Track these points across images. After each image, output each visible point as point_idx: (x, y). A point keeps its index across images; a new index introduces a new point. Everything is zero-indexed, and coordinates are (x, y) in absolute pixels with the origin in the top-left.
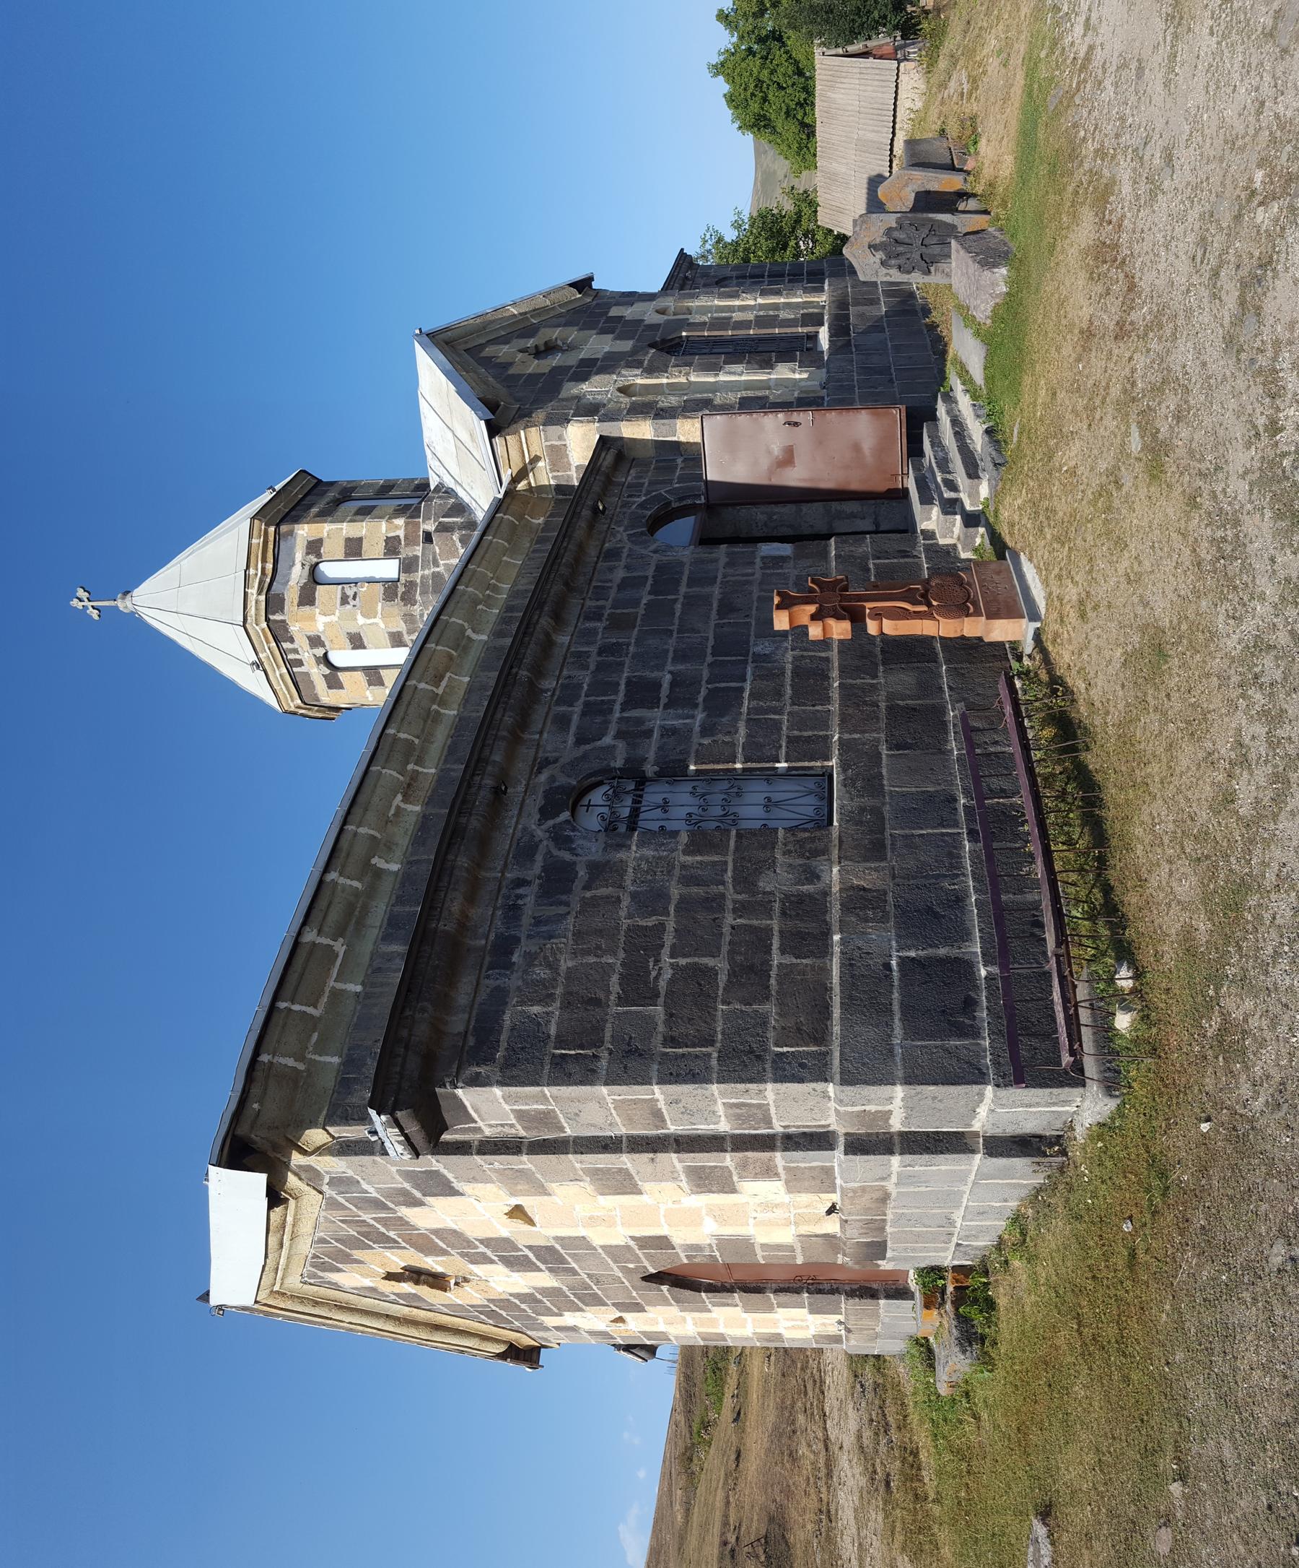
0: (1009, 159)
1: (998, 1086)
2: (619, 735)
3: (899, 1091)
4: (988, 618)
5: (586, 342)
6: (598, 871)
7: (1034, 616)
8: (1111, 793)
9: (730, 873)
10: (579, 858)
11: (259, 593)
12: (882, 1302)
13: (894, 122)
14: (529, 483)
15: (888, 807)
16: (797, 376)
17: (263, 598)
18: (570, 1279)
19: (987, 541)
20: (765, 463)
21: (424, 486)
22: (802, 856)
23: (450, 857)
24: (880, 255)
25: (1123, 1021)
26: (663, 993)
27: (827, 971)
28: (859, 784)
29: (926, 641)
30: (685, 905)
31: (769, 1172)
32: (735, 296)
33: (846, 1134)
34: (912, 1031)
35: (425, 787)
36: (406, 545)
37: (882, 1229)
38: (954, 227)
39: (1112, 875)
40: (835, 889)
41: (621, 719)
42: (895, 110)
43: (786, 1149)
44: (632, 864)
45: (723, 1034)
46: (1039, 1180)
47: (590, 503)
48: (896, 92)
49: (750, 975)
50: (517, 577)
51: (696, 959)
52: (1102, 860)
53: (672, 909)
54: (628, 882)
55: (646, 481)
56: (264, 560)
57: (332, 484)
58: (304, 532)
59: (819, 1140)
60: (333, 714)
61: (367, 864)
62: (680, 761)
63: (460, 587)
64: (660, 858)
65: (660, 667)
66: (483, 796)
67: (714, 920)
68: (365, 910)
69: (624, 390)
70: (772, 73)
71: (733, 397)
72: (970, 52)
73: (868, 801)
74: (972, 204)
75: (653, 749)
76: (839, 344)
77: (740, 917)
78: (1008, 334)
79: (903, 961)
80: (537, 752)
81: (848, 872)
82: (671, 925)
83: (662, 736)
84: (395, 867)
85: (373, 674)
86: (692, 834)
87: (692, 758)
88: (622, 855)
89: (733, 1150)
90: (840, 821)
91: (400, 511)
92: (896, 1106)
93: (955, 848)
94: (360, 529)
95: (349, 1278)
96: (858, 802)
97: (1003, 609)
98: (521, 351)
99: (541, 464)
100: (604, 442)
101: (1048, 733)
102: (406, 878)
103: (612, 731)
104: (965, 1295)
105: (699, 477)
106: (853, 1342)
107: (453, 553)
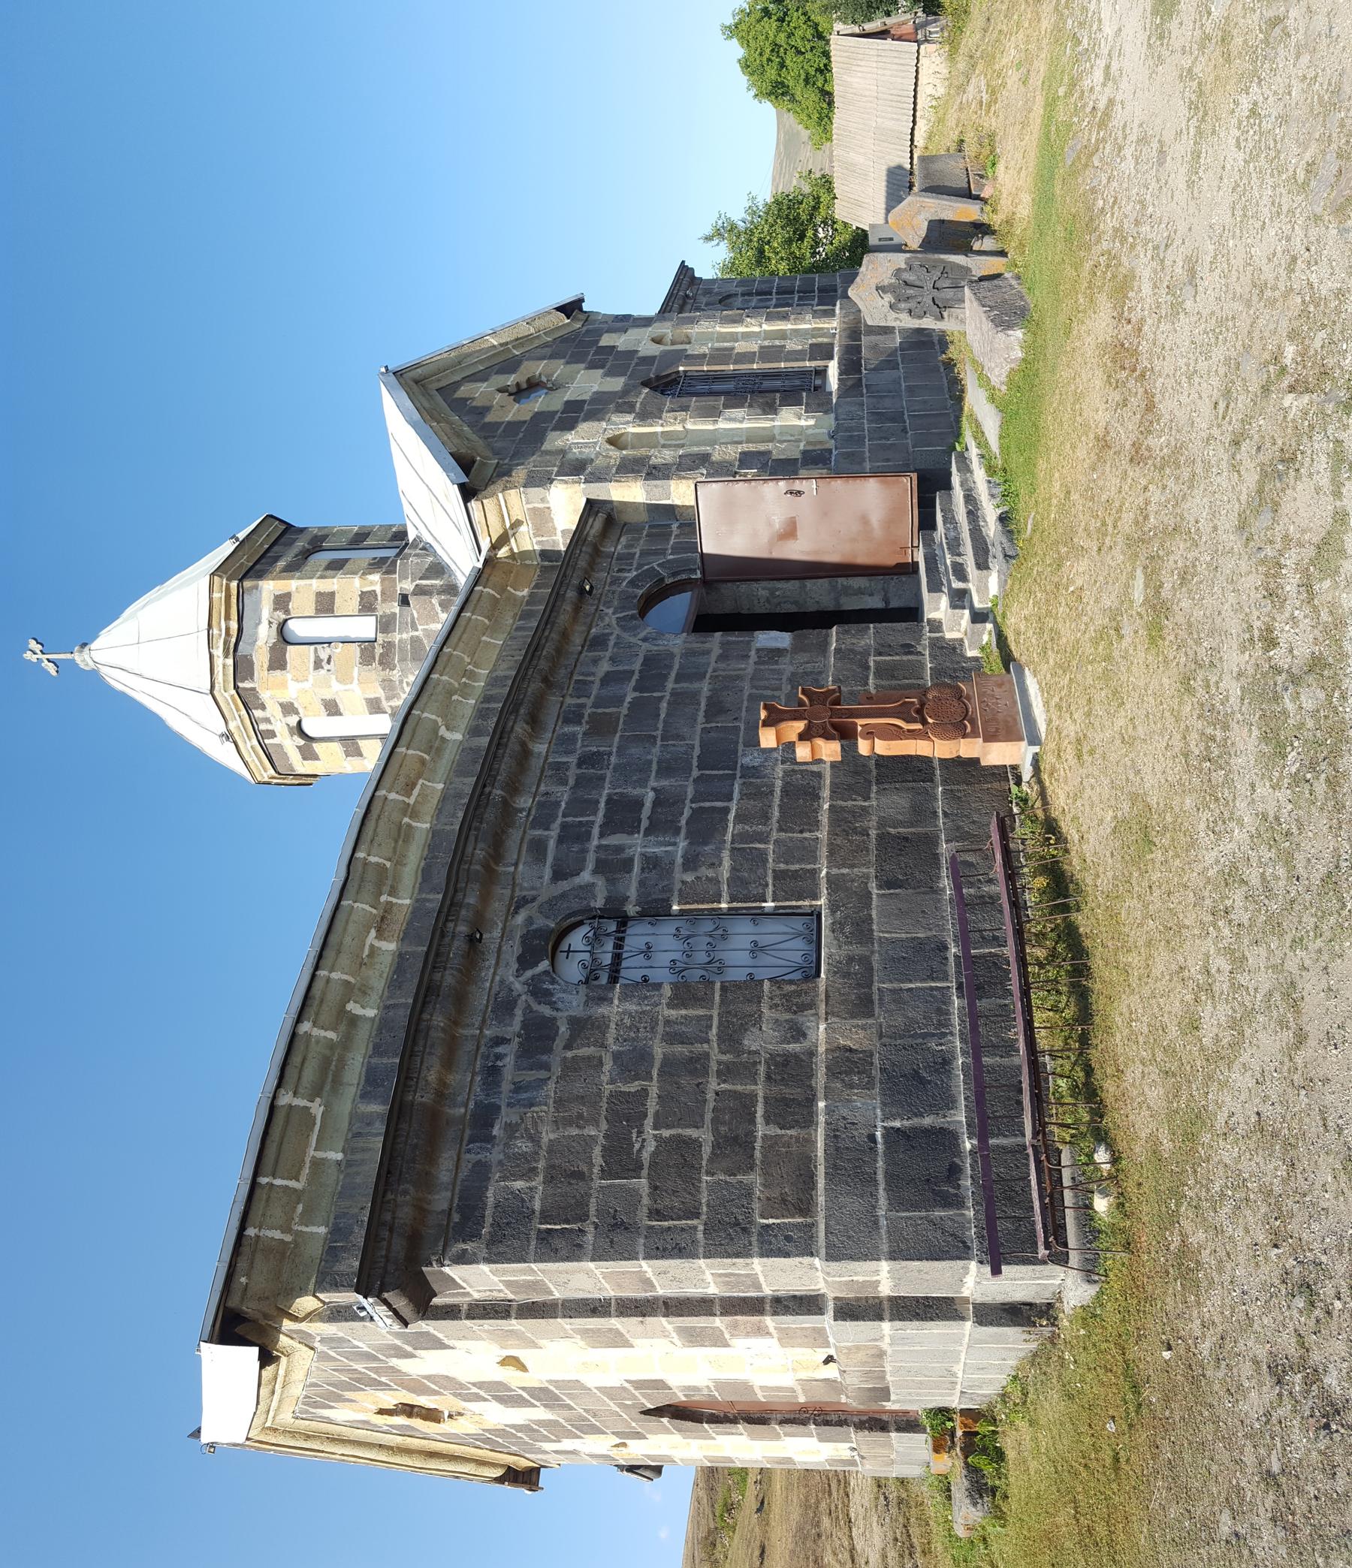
0: (1026, 198)
1: (981, 1262)
3: (884, 1266)
4: (985, 741)
5: (573, 379)
6: (578, 1026)
7: (1034, 740)
8: (1096, 963)
9: (714, 1031)
10: (560, 1014)
11: (226, 656)
12: (893, 1435)
13: (915, 110)
14: (511, 549)
15: (876, 957)
16: (803, 423)
17: (230, 661)
18: (566, 1413)
19: (994, 639)
20: (764, 536)
21: (402, 534)
22: (789, 1010)
23: (425, 1016)
24: (889, 298)
25: (1101, 1204)
27: (813, 1143)
28: (847, 929)
29: (927, 761)
31: (761, 1331)
32: (737, 321)
33: (836, 1299)
34: (897, 1202)
35: (399, 921)
36: (384, 601)
37: (883, 1378)
38: (968, 270)
39: (1094, 1055)
40: (822, 1049)
41: (599, 847)
42: (915, 97)
43: (775, 1313)
44: (614, 1019)
45: (708, 1206)
46: (1033, 1346)
47: (575, 582)
48: (916, 78)
49: (735, 1146)
50: (497, 660)
51: (680, 1131)
52: (1084, 1040)
53: (655, 1073)
54: (610, 1041)
55: (637, 551)
56: (228, 618)
57: (302, 530)
58: (269, 587)
59: (807, 1304)
60: (309, 780)
61: (342, 1012)
62: (663, 900)
63: (434, 676)
64: (643, 1012)
66: (457, 947)
67: (698, 1085)
68: (342, 1063)
69: (613, 441)
70: (789, 37)
71: (732, 453)
72: (990, 59)
73: (857, 950)
74: (988, 243)
75: (634, 885)
76: (850, 383)
77: (725, 1081)
78: (1023, 397)
79: (889, 1132)
80: (513, 891)
81: (834, 1030)
82: (654, 1091)
84: (371, 1013)
85: (351, 745)
86: (675, 986)
87: (675, 898)
88: (603, 1010)
89: (722, 1314)
90: (828, 971)
91: (377, 565)
92: (884, 1277)
93: (945, 1003)
94: (332, 584)
95: (341, 1413)
97: (1001, 731)
98: (500, 390)
99: (523, 529)
100: (592, 506)
101: (1041, 882)
102: (383, 1024)
104: (972, 1437)
105: (693, 547)
106: (868, 1467)
107: (434, 619)
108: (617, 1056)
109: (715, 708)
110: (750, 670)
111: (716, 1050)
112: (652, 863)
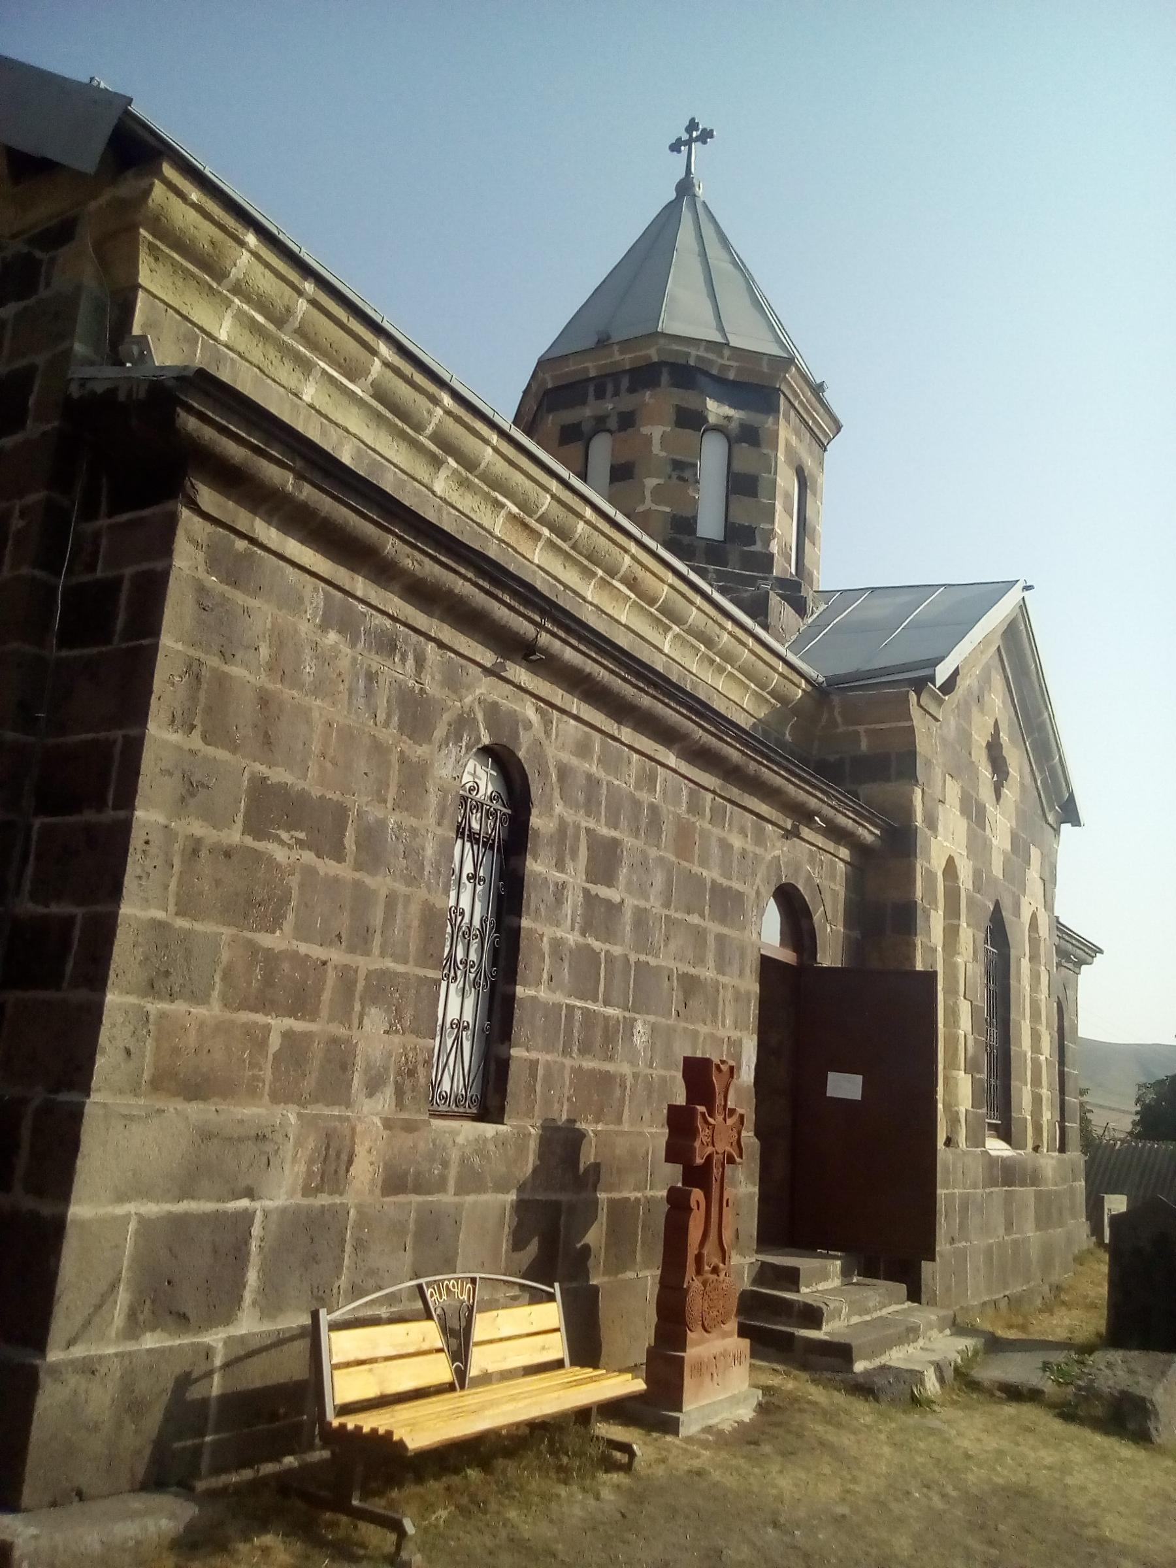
2: (563, 827)
6: (415, 776)
26: (261, 846)
30: (362, 897)
53: (357, 875)
65: (629, 891)
67: (339, 936)
83: (557, 884)
96: (454, 1156)
108: (382, 823)
109: (690, 985)
110: (722, 1033)
111: (372, 967)
112: (561, 887)
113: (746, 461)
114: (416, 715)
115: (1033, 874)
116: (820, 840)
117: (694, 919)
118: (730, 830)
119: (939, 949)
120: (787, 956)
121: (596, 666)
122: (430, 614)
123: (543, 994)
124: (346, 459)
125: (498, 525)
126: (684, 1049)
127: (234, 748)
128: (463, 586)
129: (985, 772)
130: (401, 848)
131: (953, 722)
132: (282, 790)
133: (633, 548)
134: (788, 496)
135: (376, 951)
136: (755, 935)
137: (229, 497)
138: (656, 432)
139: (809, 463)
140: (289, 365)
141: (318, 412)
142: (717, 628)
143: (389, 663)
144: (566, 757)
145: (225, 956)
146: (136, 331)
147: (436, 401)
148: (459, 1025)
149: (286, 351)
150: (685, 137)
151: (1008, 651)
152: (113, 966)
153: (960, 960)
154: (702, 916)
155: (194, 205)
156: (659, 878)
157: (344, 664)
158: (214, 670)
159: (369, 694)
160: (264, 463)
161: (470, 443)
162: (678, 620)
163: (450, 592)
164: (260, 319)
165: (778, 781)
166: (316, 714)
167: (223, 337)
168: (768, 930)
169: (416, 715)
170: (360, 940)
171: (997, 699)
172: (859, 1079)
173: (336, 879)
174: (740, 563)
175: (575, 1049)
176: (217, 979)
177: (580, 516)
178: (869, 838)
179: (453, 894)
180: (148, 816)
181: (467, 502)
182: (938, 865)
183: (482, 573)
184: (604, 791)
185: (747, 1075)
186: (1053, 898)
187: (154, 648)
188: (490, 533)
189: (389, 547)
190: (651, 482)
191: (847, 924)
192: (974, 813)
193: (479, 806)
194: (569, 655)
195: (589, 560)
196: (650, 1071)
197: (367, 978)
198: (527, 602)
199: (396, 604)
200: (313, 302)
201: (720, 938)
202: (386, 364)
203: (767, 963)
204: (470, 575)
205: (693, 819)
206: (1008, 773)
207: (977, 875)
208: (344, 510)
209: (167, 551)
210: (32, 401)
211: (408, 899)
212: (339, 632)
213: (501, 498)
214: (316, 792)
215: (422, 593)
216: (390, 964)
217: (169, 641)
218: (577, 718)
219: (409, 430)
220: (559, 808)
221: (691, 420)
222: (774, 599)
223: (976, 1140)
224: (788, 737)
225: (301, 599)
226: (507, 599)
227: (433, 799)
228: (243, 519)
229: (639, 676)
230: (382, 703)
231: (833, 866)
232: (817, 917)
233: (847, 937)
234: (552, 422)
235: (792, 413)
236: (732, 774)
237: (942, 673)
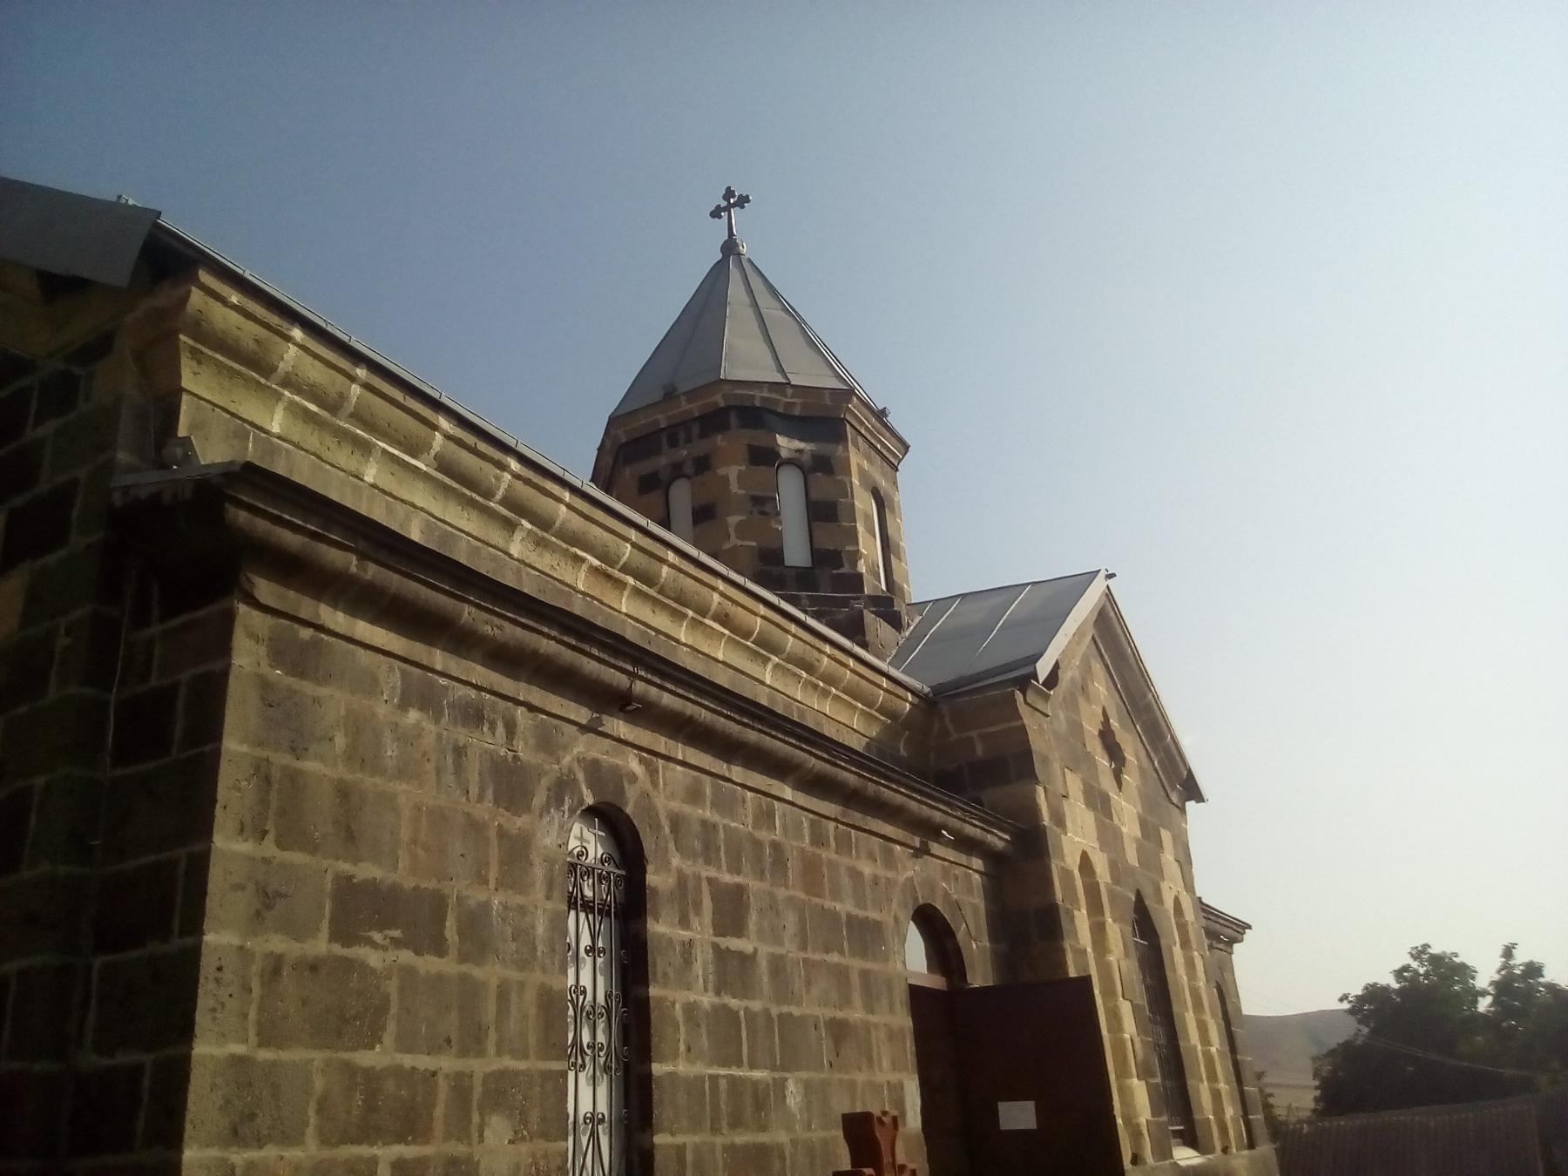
6: (517, 850)
30: (470, 991)
53: (464, 968)
67: (449, 1041)
103: (689, 867)
108: (485, 906)
109: (840, 1031)
113: (823, 488)
114: (511, 785)
115: (1168, 857)
116: (951, 854)
117: (834, 958)
118: (858, 857)
119: (1089, 950)
120: (936, 982)
121: (696, 708)
122: (516, 678)
123: (682, 1068)
124: (415, 535)
125: (581, 580)
126: (842, 1105)
127: (313, 849)
128: (547, 645)
129: (1103, 761)
130: (509, 931)
131: (1062, 716)
132: (371, 887)
133: (721, 585)
134: (868, 518)
135: (491, 1049)
136: (899, 965)
137: (288, 586)
138: (732, 472)
139: (883, 484)
140: (347, 450)
141: (384, 492)
142: (816, 654)
143: (477, 734)
144: (675, 805)
145: (319, 1084)
146: (182, 433)
147: (503, 467)
148: (594, 1119)
149: (343, 436)
150: (724, 204)
151: (1102, 637)
152: (189, 1116)
153: (1112, 958)
154: (842, 953)
155: (234, 307)
156: (791, 920)
157: (428, 741)
158: (285, 768)
159: (459, 769)
160: (323, 548)
161: (542, 503)
162: (776, 650)
163: (535, 653)
164: (313, 407)
165: (899, 799)
166: (402, 799)
167: (276, 429)
168: (913, 956)
169: (511, 785)
170: (472, 1042)
171: (1101, 688)
172: (1030, 1105)
173: (440, 978)
174: (832, 587)
175: (724, 1123)
176: (311, 1112)
177: (663, 561)
178: (1000, 845)
179: (571, 972)
180: (218, 939)
181: (545, 561)
182: (1073, 862)
183: (566, 629)
184: (722, 835)
185: (913, 1120)
186: (1192, 879)
187: (216, 755)
188: (574, 588)
189: (466, 614)
190: (733, 520)
191: (994, 936)
192: (1099, 803)
193: (589, 871)
194: (667, 700)
195: (678, 603)
196: (807, 1135)
197: (485, 1081)
198: (616, 652)
199: (480, 673)
200: (367, 386)
201: (865, 974)
202: (448, 437)
203: (917, 995)
204: (554, 633)
205: (818, 851)
206: (1124, 759)
207: (1114, 866)
208: (415, 585)
209: (223, 647)
210: (75, 513)
211: (522, 985)
212: (420, 709)
213: (580, 553)
214: (409, 883)
215: (506, 659)
216: (508, 1063)
217: (233, 745)
218: (683, 764)
219: (478, 498)
220: (676, 861)
221: (765, 457)
222: (869, 617)
223: (1164, 1153)
224: (903, 753)
225: (375, 681)
226: (595, 652)
227: (539, 872)
228: (306, 606)
229: (742, 711)
230: (474, 778)
231: (968, 877)
232: (960, 936)
233: (996, 954)
234: (629, 474)
235: (860, 439)
236: (851, 798)
237: (1043, 668)
